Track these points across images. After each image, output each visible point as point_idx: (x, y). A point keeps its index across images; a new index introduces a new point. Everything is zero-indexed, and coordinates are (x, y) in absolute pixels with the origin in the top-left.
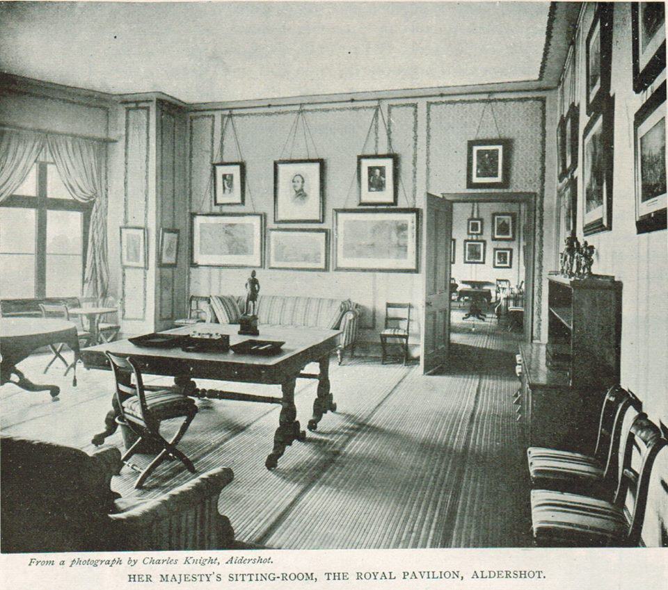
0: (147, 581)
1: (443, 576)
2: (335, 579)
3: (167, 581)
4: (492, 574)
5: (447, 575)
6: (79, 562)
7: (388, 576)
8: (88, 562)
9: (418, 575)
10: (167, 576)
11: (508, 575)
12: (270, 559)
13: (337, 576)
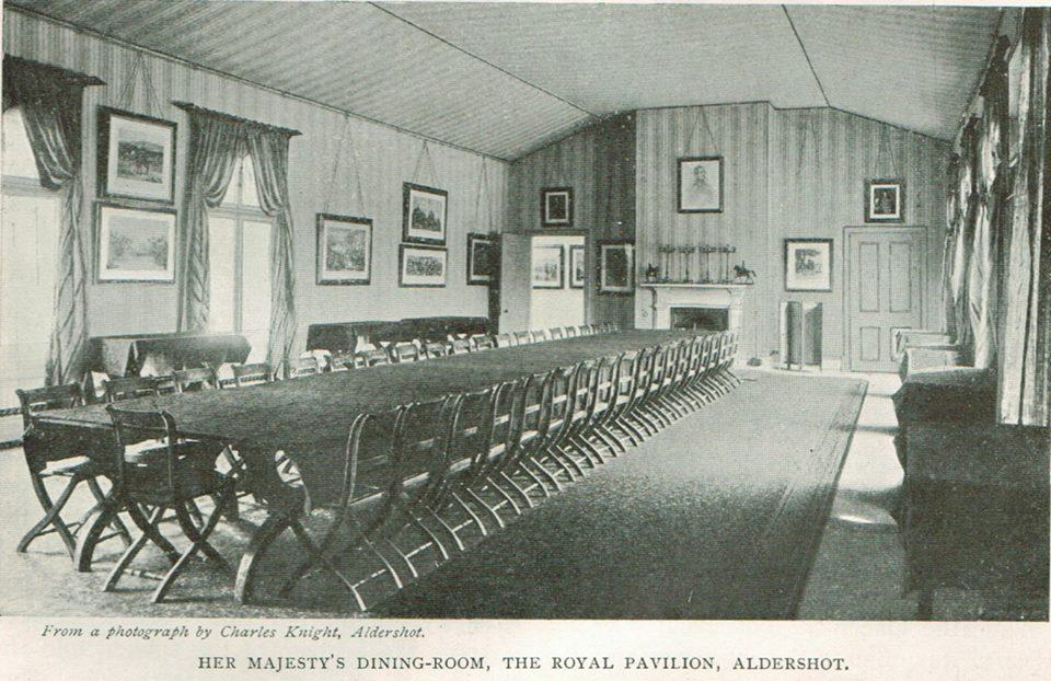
1: (688, 665)
4: (765, 664)
5: (695, 663)
7: (602, 664)
9: (649, 663)
10: (259, 659)
12: (420, 630)
13: (521, 663)
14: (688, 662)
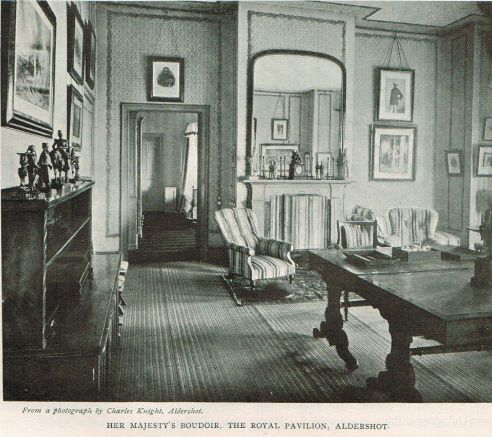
0: (121, 427)
1: (314, 427)
2: (235, 427)
3: (136, 427)
4: (351, 426)
5: (318, 426)
6: (60, 411)
7: (341, 427)
8: (66, 411)
9: (296, 426)
10: (135, 424)
11: (362, 427)
12: (200, 410)
13: (236, 425)
14: (314, 425)
